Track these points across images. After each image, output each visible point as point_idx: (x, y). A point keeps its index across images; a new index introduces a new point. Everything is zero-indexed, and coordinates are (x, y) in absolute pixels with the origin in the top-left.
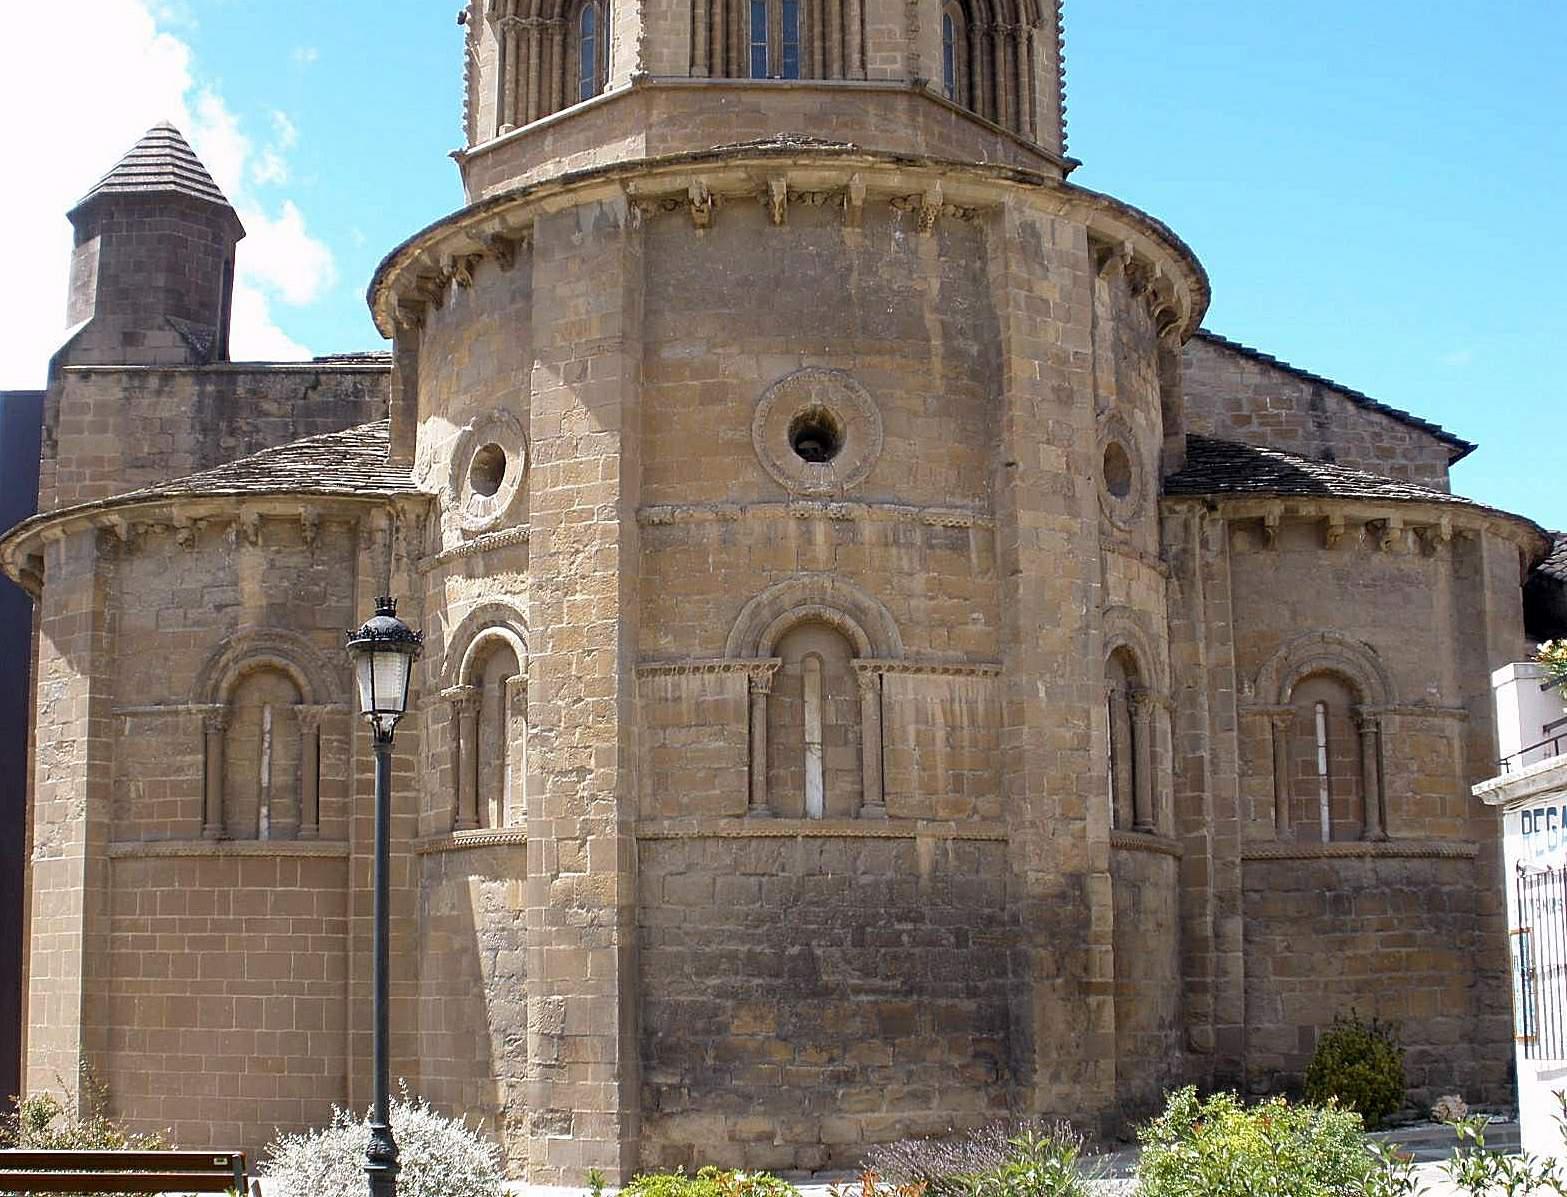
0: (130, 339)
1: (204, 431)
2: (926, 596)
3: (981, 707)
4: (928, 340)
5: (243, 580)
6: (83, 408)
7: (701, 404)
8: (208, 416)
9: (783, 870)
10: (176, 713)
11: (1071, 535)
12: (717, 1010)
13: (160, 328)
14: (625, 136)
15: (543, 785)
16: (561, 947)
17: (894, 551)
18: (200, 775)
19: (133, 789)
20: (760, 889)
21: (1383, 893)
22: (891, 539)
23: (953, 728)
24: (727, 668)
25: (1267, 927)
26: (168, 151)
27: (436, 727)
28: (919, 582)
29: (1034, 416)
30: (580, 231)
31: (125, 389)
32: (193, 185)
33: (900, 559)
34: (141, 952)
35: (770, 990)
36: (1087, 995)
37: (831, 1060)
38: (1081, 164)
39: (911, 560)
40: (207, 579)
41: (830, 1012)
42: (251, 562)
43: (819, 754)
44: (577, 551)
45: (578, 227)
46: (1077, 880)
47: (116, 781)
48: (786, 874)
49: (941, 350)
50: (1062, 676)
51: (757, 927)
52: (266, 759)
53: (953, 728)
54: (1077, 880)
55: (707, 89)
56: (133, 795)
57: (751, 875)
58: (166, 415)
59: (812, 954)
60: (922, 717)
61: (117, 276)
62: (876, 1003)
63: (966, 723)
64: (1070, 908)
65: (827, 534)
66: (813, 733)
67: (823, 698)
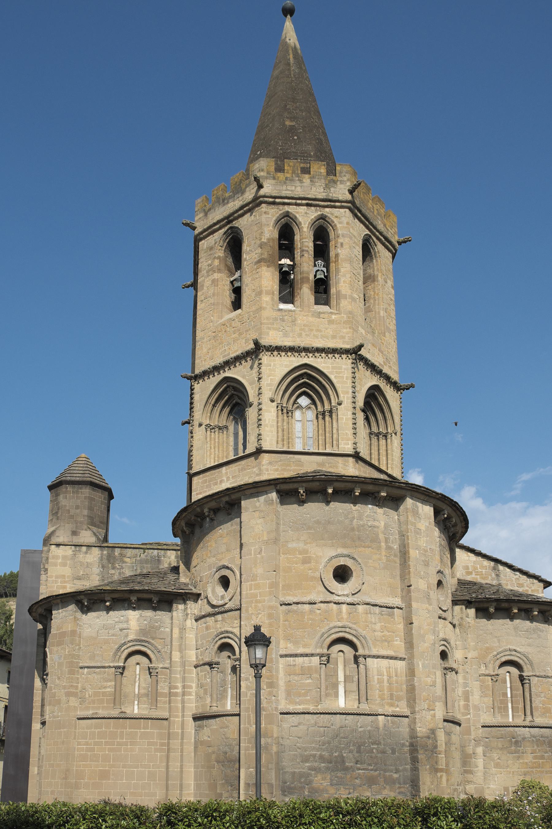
0: (74, 533)
1: (103, 567)
2: (380, 631)
3: (399, 670)
4: (380, 543)
5: (131, 620)
6: (57, 557)
7: (303, 564)
8: (105, 561)
9: (332, 726)
11: (429, 611)
12: (309, 775)
13: (86, 530)
15: (247, 694)
17: (369, 615)
18: (113, 690)
20: (324, 732)
21: (533, 740)
22: (368, 612)
23: (390, 677)
25: (491, 750)
26: (86, 466)
27: (202, 673)
28: (378, 627)
29: (417, 570)
30: (259, 502)
31: (73, 551)
32: (97, 478)
33: (372, 618)
34: (89, 753)
35: (328, 768)
36: (437, 772)
37: (349, 793)
39: (375, 618)
40: (117, 620)
41: (349, 776)
43: (343, 685)
46: (433, 731)
47: (80, 691)
48: (333, 727)
49: (385, 547)
50: (427, 660)
51: (323, 746)
52: (137, 684)
53: (390, 677)
54: (433, 731)
57: (321, 727)
58: (89, 561)
59: (342, 755)
60: (380, 673)
61: (69, 510)
62: (364, 773)
63: (394, 676)
64: (431, 741)
65: (346, 609)
66: (341, 677)
67: (345, 666)
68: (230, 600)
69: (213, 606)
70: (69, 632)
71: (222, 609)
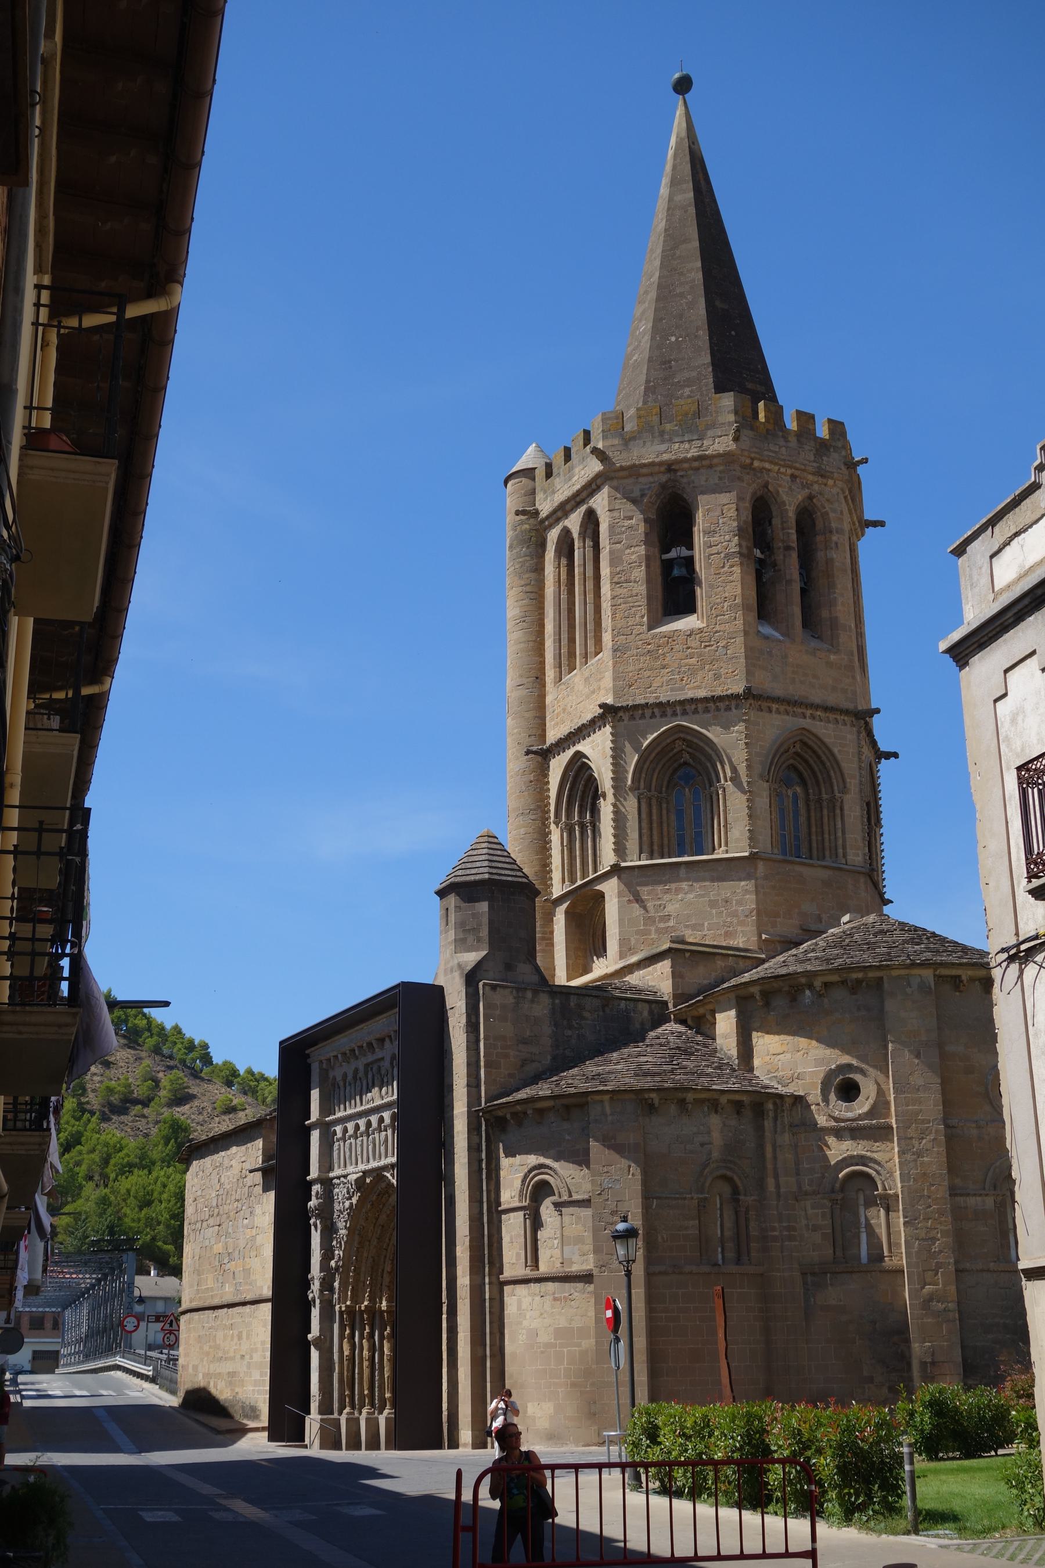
1: (556, 1025)
10: (685, 1199)
14: (740, 880)
16: (929, 1320)
19: (660, 1238)
24: (987, 1195)
31: (515, 998)
38: (892, 902)
42: (715, 1120)
44: (923, 1138)
45: (909, 985)
55: (780, 861)
56: (660, 1239)
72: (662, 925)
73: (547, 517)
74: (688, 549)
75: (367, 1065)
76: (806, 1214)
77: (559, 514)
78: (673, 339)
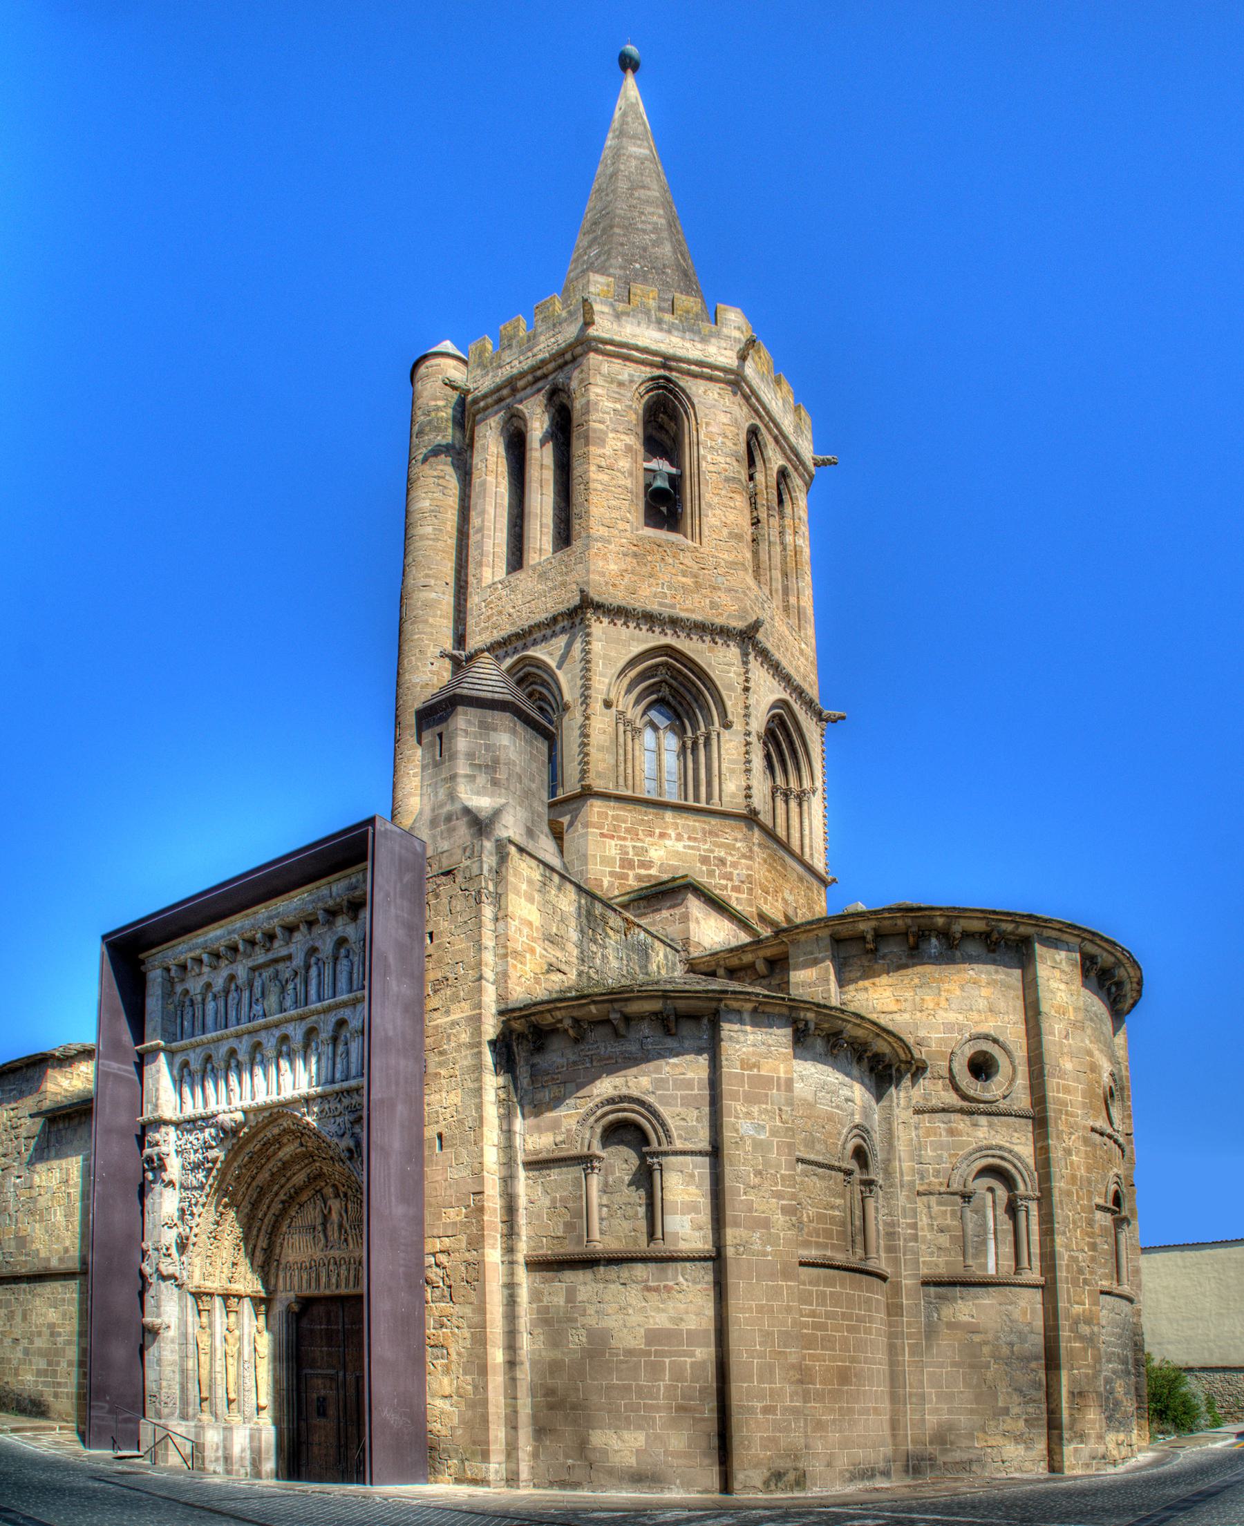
44: (1071, 1133)
68: (1005, 1097)
69: (965, 1097)
70: (782, 1081)
71: (994, 1109)
72: (643, 872)
73: (485, 397)
74: (672, 465)
75: (253, 969)
76: (930, 1212)
77: (505, 392)
78: (638, 266)
